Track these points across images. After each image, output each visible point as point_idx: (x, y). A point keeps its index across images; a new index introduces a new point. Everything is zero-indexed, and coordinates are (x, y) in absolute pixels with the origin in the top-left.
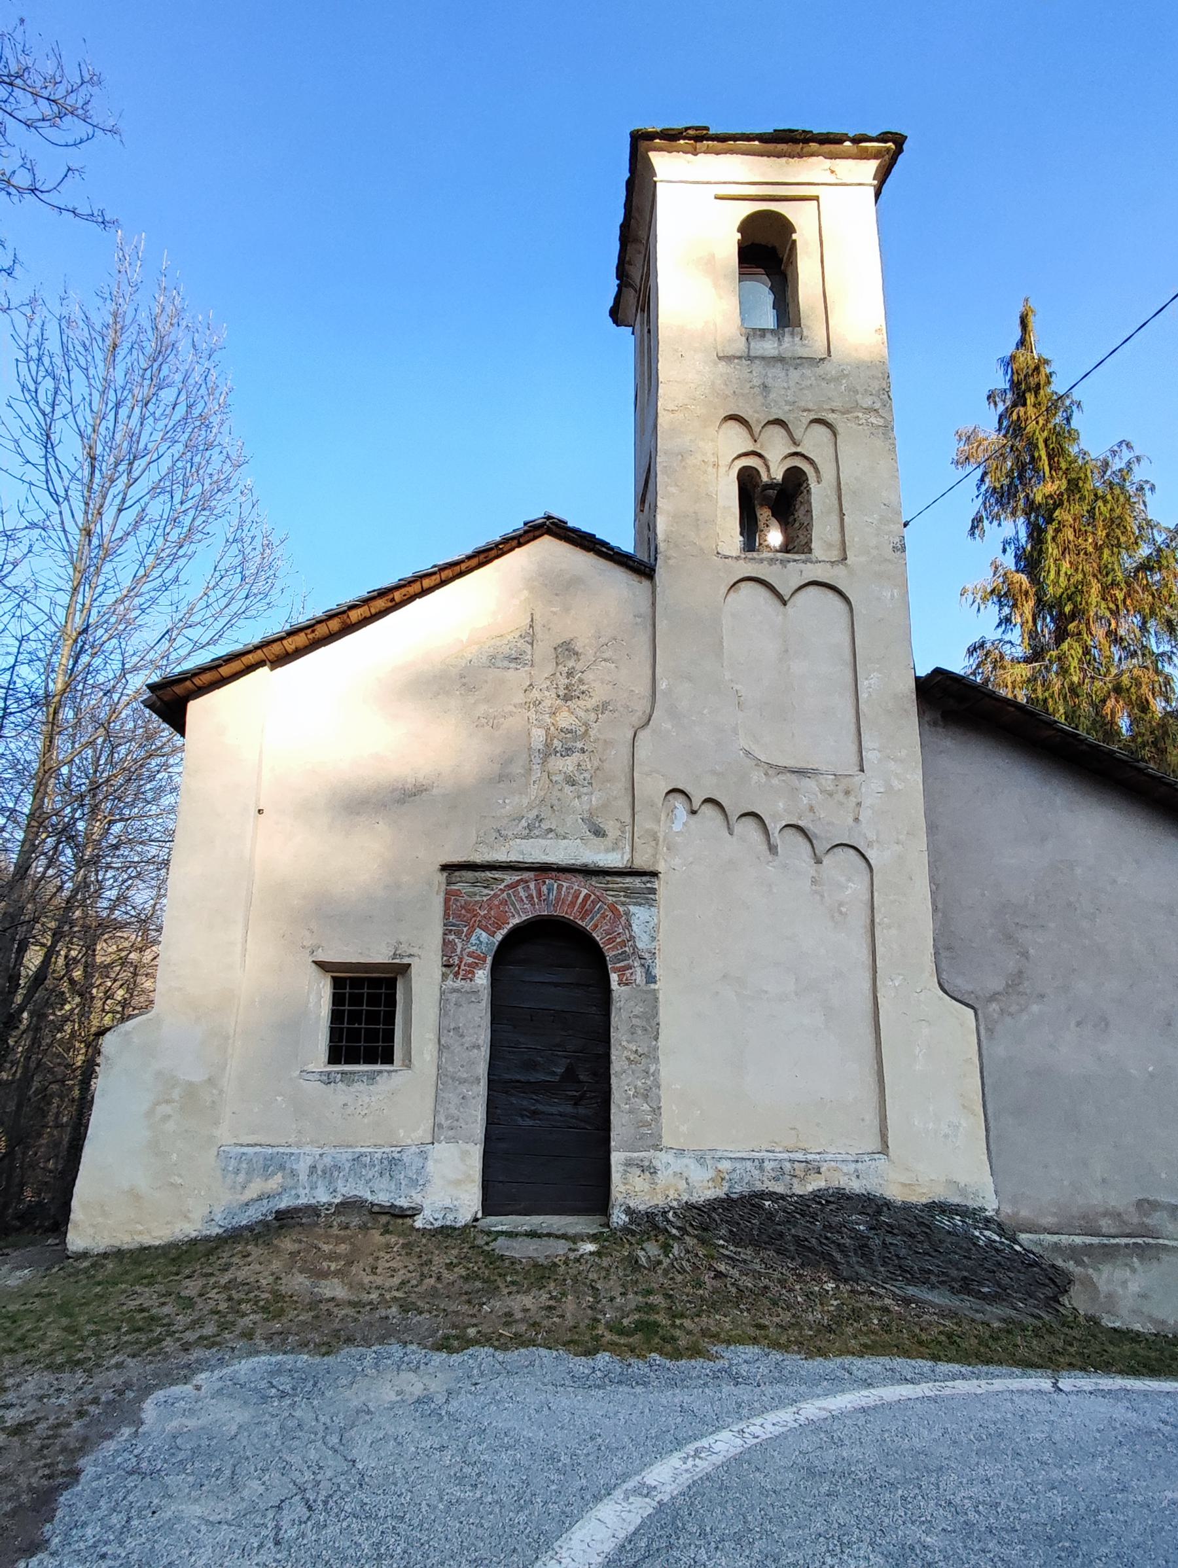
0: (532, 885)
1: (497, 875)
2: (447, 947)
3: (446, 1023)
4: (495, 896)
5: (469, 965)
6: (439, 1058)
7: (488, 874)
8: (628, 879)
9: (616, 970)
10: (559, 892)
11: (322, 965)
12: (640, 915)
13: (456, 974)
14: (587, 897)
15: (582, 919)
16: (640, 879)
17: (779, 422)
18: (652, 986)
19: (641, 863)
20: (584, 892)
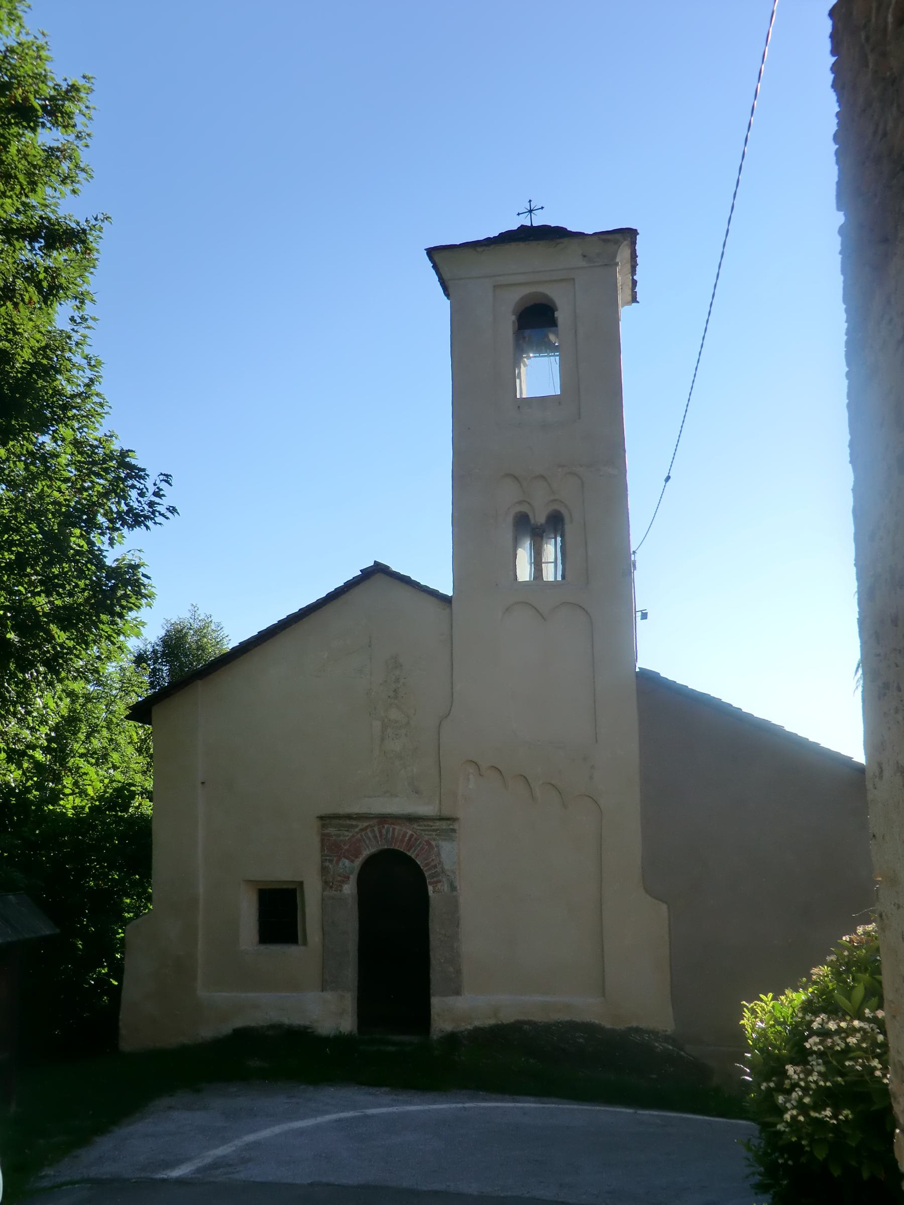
0: (376, 829)
1: (354, 823)
2: (324, 870)
3: (330, 911)
4: (353, 836)
5: (339, 882)
6: (324, 939)
7: (348, 822)
8: (438, 823)
9: (431, 883)
10: (393, 833)
11: (248, 882)
12: (446, 849)
13: (331, 887)
14: (412, 836)
15: (409, 851)
16: (446, 824)
17: (542, 477)
18: (455, 893)
19: (446, 813)
20: (410, 832)
